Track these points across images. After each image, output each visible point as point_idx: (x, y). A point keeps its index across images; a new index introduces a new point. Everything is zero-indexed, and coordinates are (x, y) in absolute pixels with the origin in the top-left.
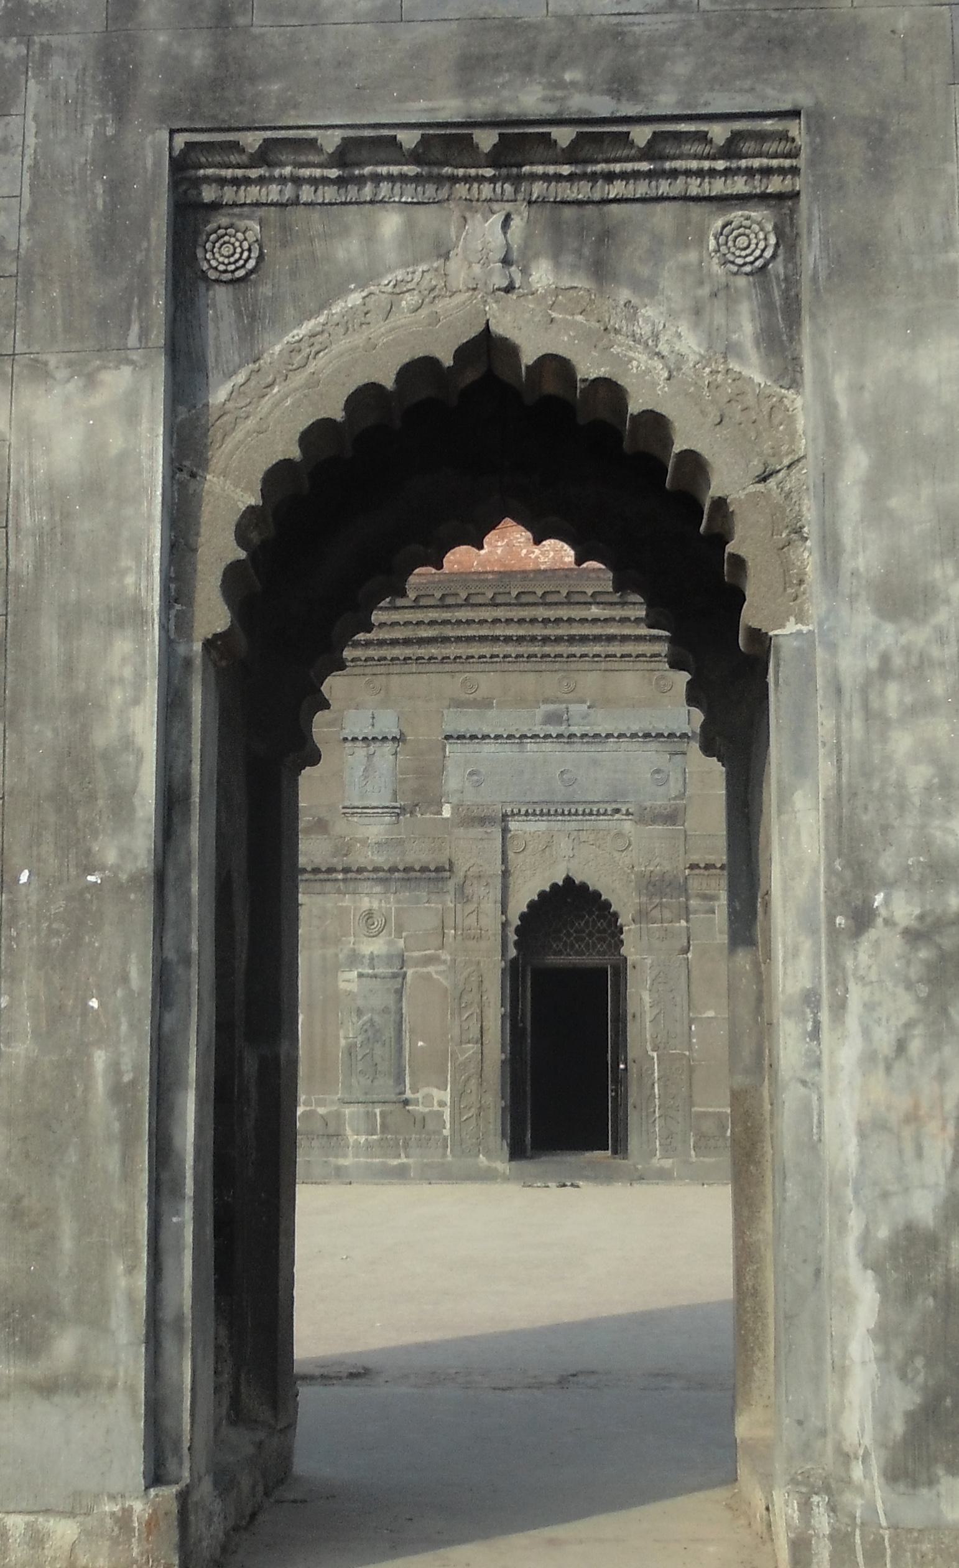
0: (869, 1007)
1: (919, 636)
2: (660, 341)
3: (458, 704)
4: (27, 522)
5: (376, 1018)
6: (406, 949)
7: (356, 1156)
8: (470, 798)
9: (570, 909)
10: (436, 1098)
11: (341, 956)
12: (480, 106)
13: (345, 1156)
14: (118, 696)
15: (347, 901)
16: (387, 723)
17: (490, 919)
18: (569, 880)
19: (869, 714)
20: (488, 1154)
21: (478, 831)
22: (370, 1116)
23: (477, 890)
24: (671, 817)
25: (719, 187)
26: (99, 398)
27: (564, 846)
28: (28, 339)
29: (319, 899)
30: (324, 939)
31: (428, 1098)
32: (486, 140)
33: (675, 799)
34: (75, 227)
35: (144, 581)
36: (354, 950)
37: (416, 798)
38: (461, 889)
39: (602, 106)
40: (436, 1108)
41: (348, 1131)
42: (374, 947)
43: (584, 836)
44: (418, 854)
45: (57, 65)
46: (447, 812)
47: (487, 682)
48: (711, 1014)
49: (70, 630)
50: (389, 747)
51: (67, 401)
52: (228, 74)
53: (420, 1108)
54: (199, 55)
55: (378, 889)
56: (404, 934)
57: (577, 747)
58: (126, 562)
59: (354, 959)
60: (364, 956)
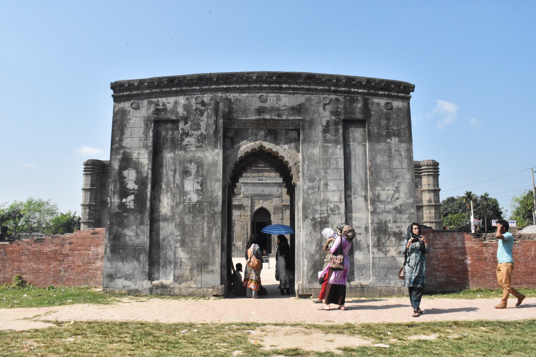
0: (307, 228)
1: (314, 184)
2: (284, 150)
4: (205, 168)
8: (245, 193)
12: (261, 117)
14: (217, 190)
17: (249, 213)
18: (262, 207)
19: (307, 193)
21: (247, 199)
24: (279, 197)
25: (290, 128)
26: (214, 153)
28: (205, 145)
32: (262, 122)
34: (212, 132)
35: (220, 176)
39: (276, 118)
45: (209, 110)
46: (242, 195)
49: (211, 182)
51: (210, 153)
52: (231, 112)
54: (227, 110)
58: (218, 173)
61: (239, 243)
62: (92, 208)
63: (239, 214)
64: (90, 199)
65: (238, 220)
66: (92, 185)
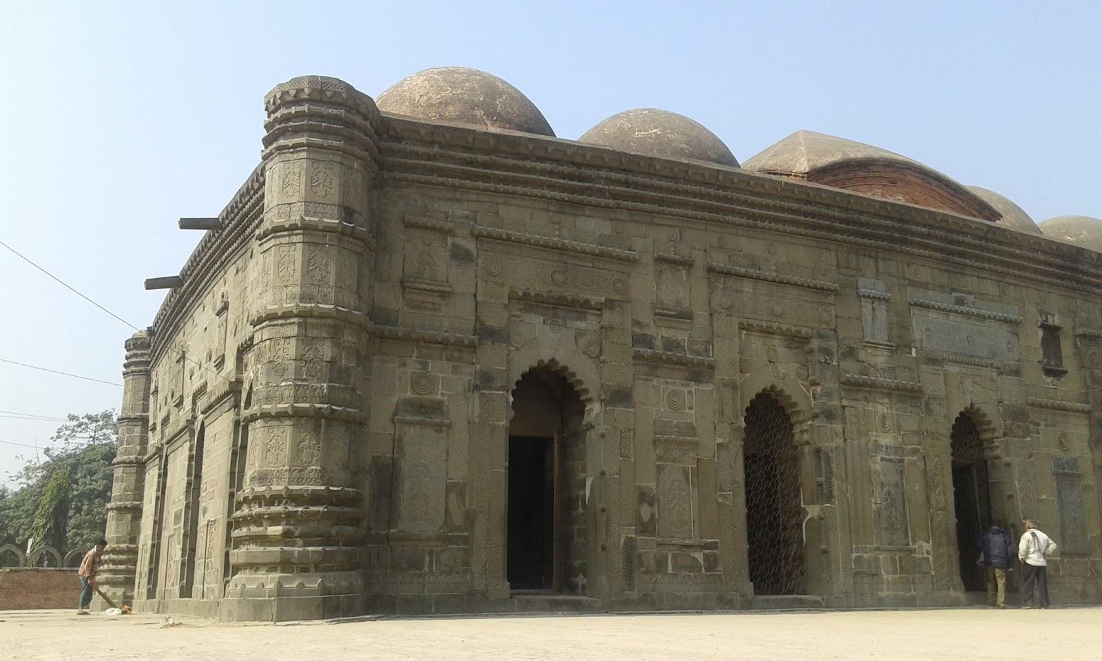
3: (913, 284)
5: (892, 491)
6: (903, 443)
7: (888, 589)
9: (968, 428)
10: (924, 548)
11: (869, 445)
13: (882, 590)
15: (870, 407)
16: (879, 289)
20: (954, 589)
21: (931, 368)
22: (893, 560)
23: (935, 407)
24: (1017, 373)
27: (968, 382)
29: (854, 403)
30: (859, 433)
31: (920, 547)
33: (1017, 361)
36: (875, 441)
37: (899, 344)
38: (927, 404)
40: (926, 555)
41: (883, 572)
42: (886, 440)
43: (977, 379)
44: (903, 380)
46: (914, 354)
47: (924, 273)
48: (1044, 497)
50: (883, 306)
53: (917, 555)
55: (886, 400)
56: (902, 433)
57: (973, 321)
59: (877, 447)
60: (882, 446)
61: (927, 546)
62: (348, 338)
63: (915, 428)
64: (338, 287)
65: (915, 452)
66: (348, 213)
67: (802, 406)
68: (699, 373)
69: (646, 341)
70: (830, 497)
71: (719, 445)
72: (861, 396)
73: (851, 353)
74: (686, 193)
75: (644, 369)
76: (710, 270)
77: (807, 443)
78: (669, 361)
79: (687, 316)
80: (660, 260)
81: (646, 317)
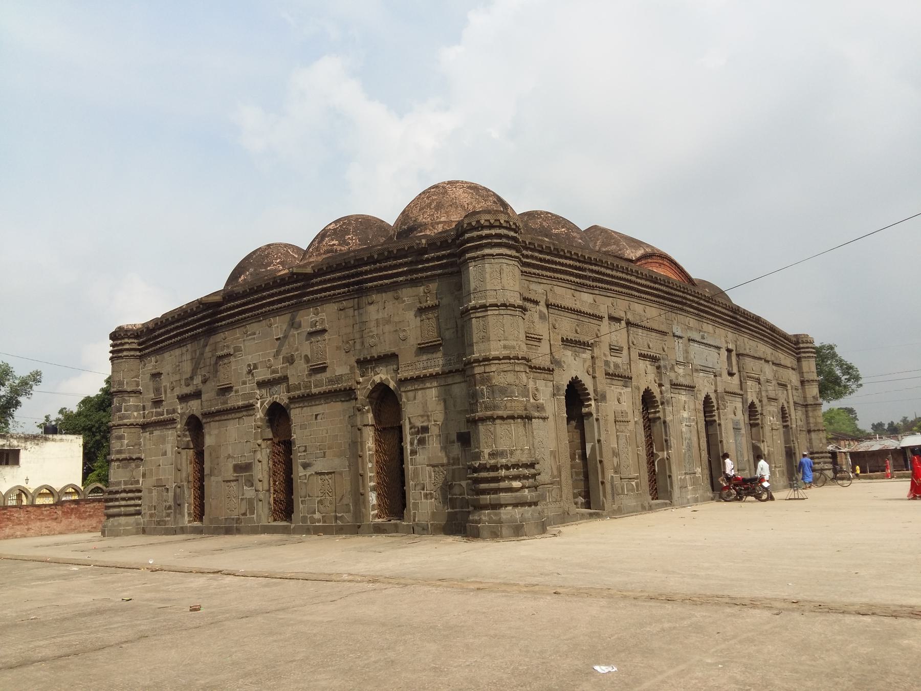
42: (686, 415)
67: (658, 397)
68: (626, 379)
69: (607, 363)
70: (668, 447)
71: (636, 422)
72: (677, 391)
73: (672, 368)
74: (617, 278)
75: (609, 381)
76: (629, 323)
77: (659, 418)
78: (618, 376)
79: (620, 350)
80: (612, 318)
81: (608, 353)
